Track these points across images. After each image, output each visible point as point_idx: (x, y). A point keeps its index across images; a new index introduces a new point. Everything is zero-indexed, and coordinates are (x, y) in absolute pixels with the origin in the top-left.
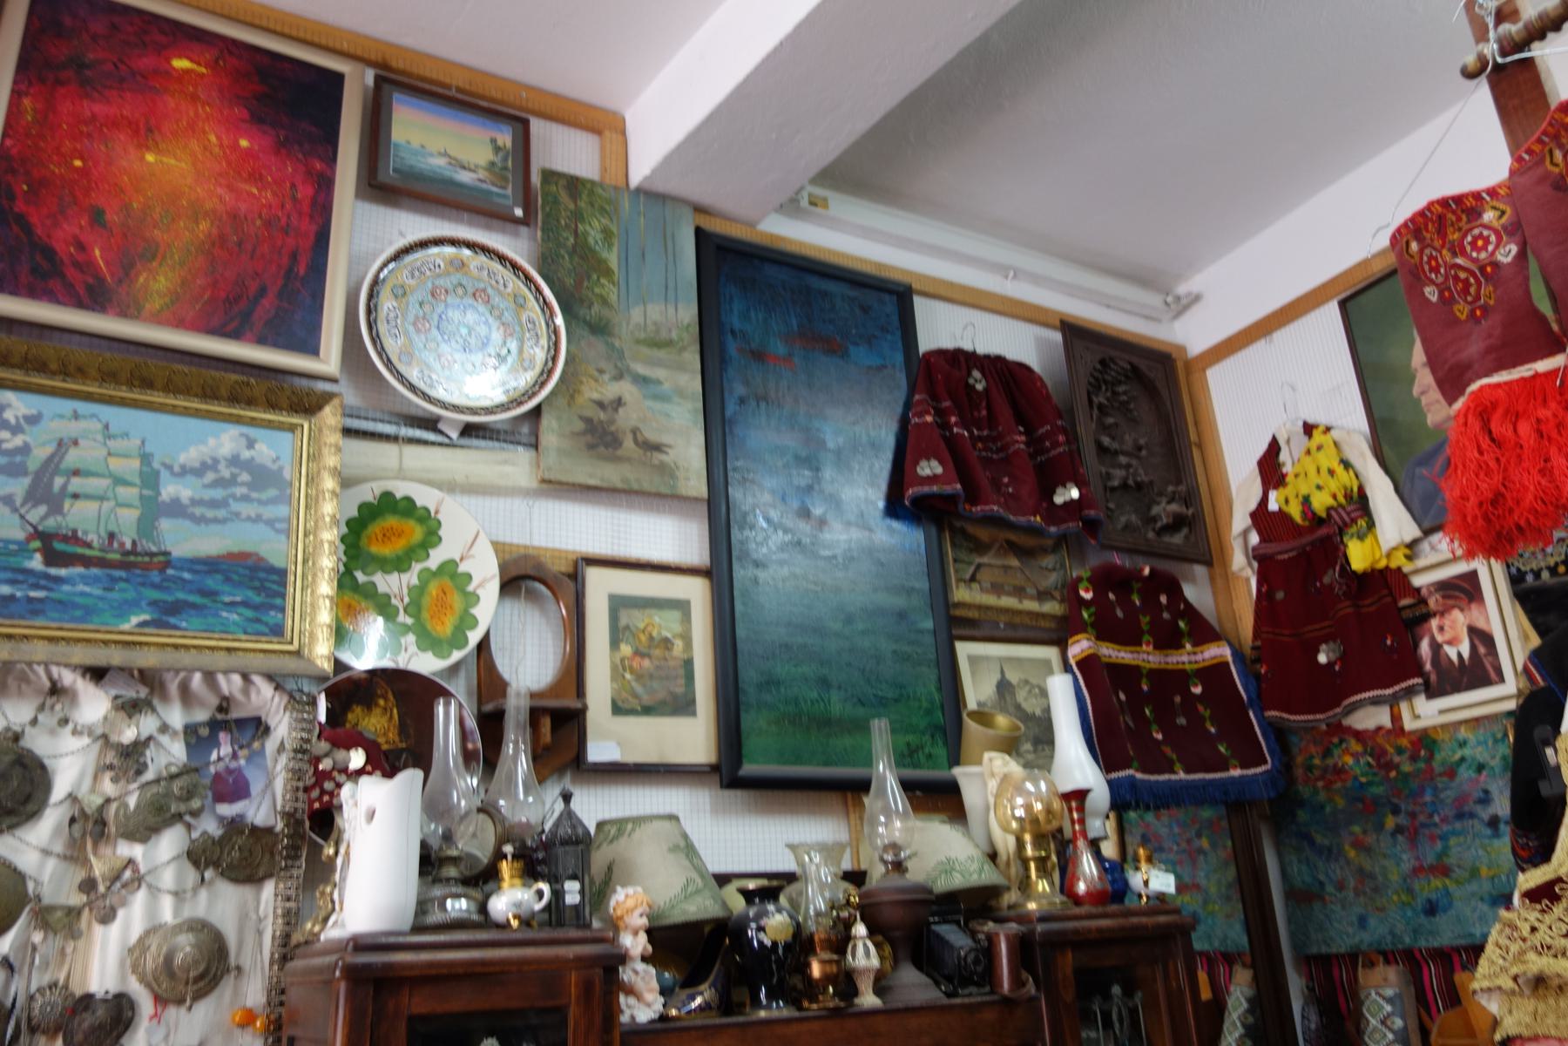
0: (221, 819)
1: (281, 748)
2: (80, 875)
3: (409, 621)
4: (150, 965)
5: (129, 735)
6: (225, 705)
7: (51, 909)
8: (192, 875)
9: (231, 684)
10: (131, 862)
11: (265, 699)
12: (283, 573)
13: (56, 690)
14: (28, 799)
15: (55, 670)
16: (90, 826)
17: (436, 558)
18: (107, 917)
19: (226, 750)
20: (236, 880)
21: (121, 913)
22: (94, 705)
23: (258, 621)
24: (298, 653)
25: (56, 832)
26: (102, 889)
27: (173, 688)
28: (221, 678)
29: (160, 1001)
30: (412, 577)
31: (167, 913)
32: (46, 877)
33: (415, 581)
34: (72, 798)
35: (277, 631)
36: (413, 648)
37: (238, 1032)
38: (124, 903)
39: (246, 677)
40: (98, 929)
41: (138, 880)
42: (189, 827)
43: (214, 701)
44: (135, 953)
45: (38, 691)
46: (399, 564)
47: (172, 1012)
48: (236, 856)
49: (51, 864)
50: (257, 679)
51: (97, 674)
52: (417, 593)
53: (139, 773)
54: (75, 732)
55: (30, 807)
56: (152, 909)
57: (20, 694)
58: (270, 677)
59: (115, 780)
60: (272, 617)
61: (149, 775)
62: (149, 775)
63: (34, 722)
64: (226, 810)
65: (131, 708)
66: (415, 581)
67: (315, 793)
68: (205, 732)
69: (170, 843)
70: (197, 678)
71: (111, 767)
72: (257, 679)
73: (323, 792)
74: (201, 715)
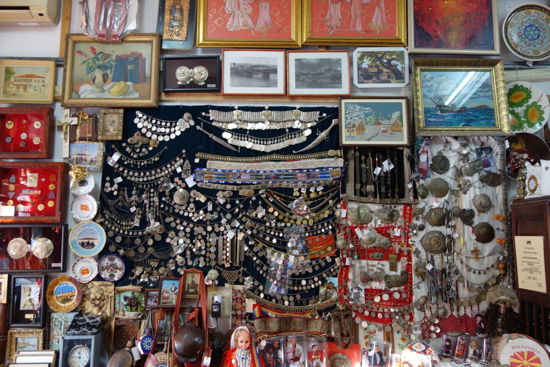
0: (486, 172)
1: (497, 154)
2: (457, 184)
3: (525, 120)
4: (477, 203)
5: (465, 152)
6: (483, 144)
7: (454, 190)
8: (481, 184)
9: (484, 139)
10: (469, 181)
11: (492, 142)
12: (493, 110)
13: (447, 142)
14: (446, 167)
15: (447, 138)
16: (459, 173)
17: (530, 102)
18: (465, 193)
19: (484, 155)
20: (491, 186)
21: (468, 192)
22: (456, 145)
23: (489, 123)
24: (500, 130)
25: (453, 173)
26: (463, 186)
27: (471, 140)
28: (481, 137)
29: (479, 211)
30: (524, 108)
31: (478, 192)
32: (452, 184)
33: (525, 109)
34: (455, 166)
35: (494, 125)
36: (527, 127)
37: (496, 220)
38: (468, 190)
39: (487, 137)
40: (463, 195)
41: (470, 185)
42: (479, 173)
43: (480, 143)
44: (474, 200)
45: (443, 143)
46: (520, 105)
47: (481, 214)
48: (491, 180)
49: (452, 181)
50: (490, 137)
51: (456, 138)
52: (526, 112)
53: (468, 160)
54: (453, 152)
55: (447, 168)
56: (475, 192)
57: (440, 143)
58: (493, 137)
59: (464, 162)
60: (492, 121)
61: (470, 161)
62: (470, 161)
63: (444, 150)
64: (486, 169)
65: (464, 146)
66: (525, 109)
67: (516, 164)
68: (479, 151)
69: (476, 177)
70: (476, 137)
71: (462, 159)
72: (490, 137)
73: (519, 164)
74: (478, 147)
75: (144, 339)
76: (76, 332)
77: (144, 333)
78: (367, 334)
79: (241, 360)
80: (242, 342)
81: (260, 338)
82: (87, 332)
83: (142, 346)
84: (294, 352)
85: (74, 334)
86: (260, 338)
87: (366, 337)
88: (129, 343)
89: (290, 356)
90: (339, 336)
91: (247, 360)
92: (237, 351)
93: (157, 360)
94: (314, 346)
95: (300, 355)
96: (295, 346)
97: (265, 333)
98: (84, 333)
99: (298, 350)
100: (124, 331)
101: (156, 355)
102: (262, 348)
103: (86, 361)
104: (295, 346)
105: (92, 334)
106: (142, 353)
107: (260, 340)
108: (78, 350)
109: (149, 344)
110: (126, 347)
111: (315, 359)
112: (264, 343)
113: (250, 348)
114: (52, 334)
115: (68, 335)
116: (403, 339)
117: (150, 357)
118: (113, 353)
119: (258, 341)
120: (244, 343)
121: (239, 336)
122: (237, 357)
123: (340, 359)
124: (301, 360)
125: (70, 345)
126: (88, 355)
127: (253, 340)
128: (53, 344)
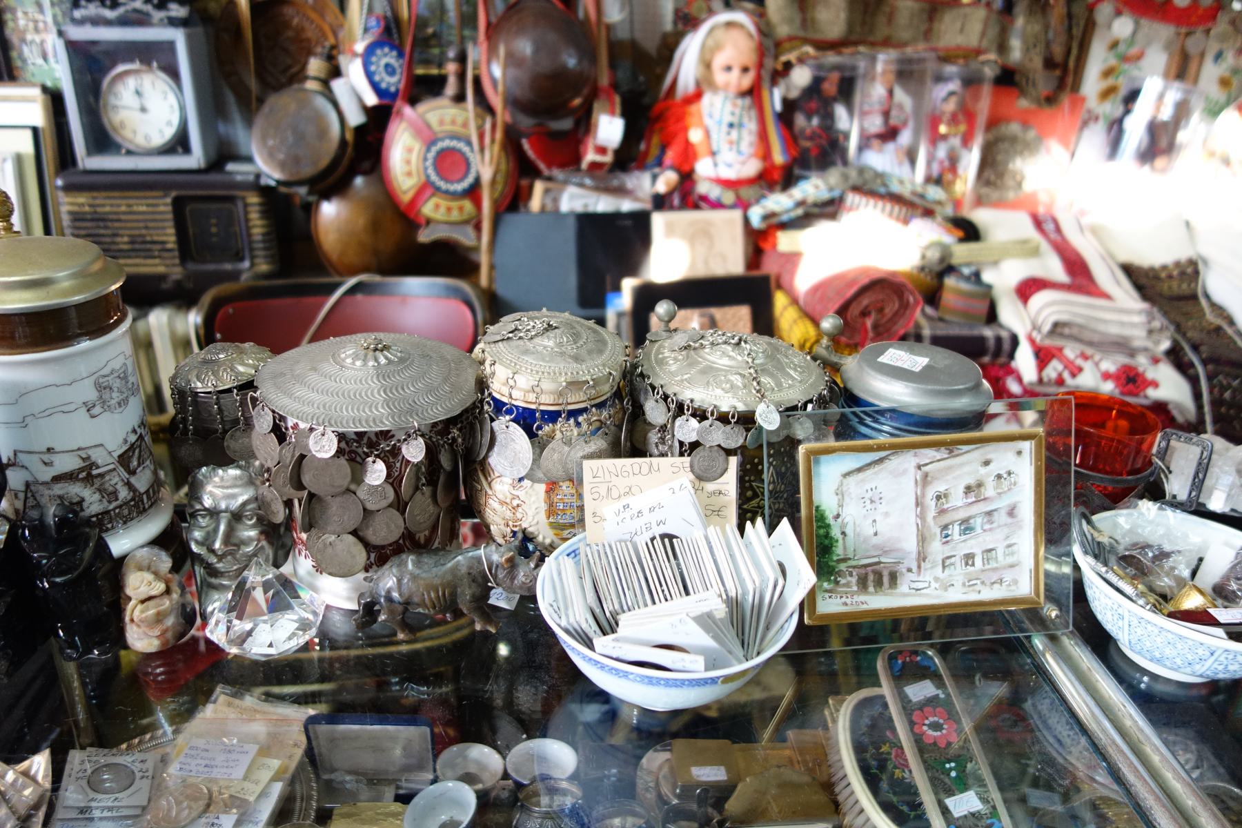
75: (370, 51)
76: (109, 14)
77: (366, 30)
78: (1112, 61)
79: (725, 128)
80: (729, 69)
81: (791, 57)
82: (147, 14)
83: (369, 75)
84: (886, 114)
85: (97, 21)
86: (791, 57)
87: (1108, 73)
88: (315, 66)
89: (875, 124)
90: (1037, 62)
91: (745, 133)
92: (707, 99)
93: (429, 126)
94: (952, 94)
95: (905, 124)
96: (891, 93)
97: (806, 41)
98: (139, 20)
99: (901, 107)
100: (287, 25)
101: (423, 107)
102: (794, 94)
103: (169, 123)
104: (891, 93)
105: (173, 22)
106: (371, 100)
107: (788, 66)
108: (131, 82)
109: (390, 70)
110: (306, 78)
111: (944, 137)
112: (801, 77)
113: (753, 93)
114: (10, 24)
115: (80, 22)
116: (1224, 82)
117: (399, 113)
118: (261, 101)
119: (780, 67)
120: (736, 73)
121: (718, 47)
122: (708, 122)
123: (1013, 140)
124: (905, 138)
125: (93, 65)
126: (172, 99)
127: (769, 63)
128: (24, 61)
